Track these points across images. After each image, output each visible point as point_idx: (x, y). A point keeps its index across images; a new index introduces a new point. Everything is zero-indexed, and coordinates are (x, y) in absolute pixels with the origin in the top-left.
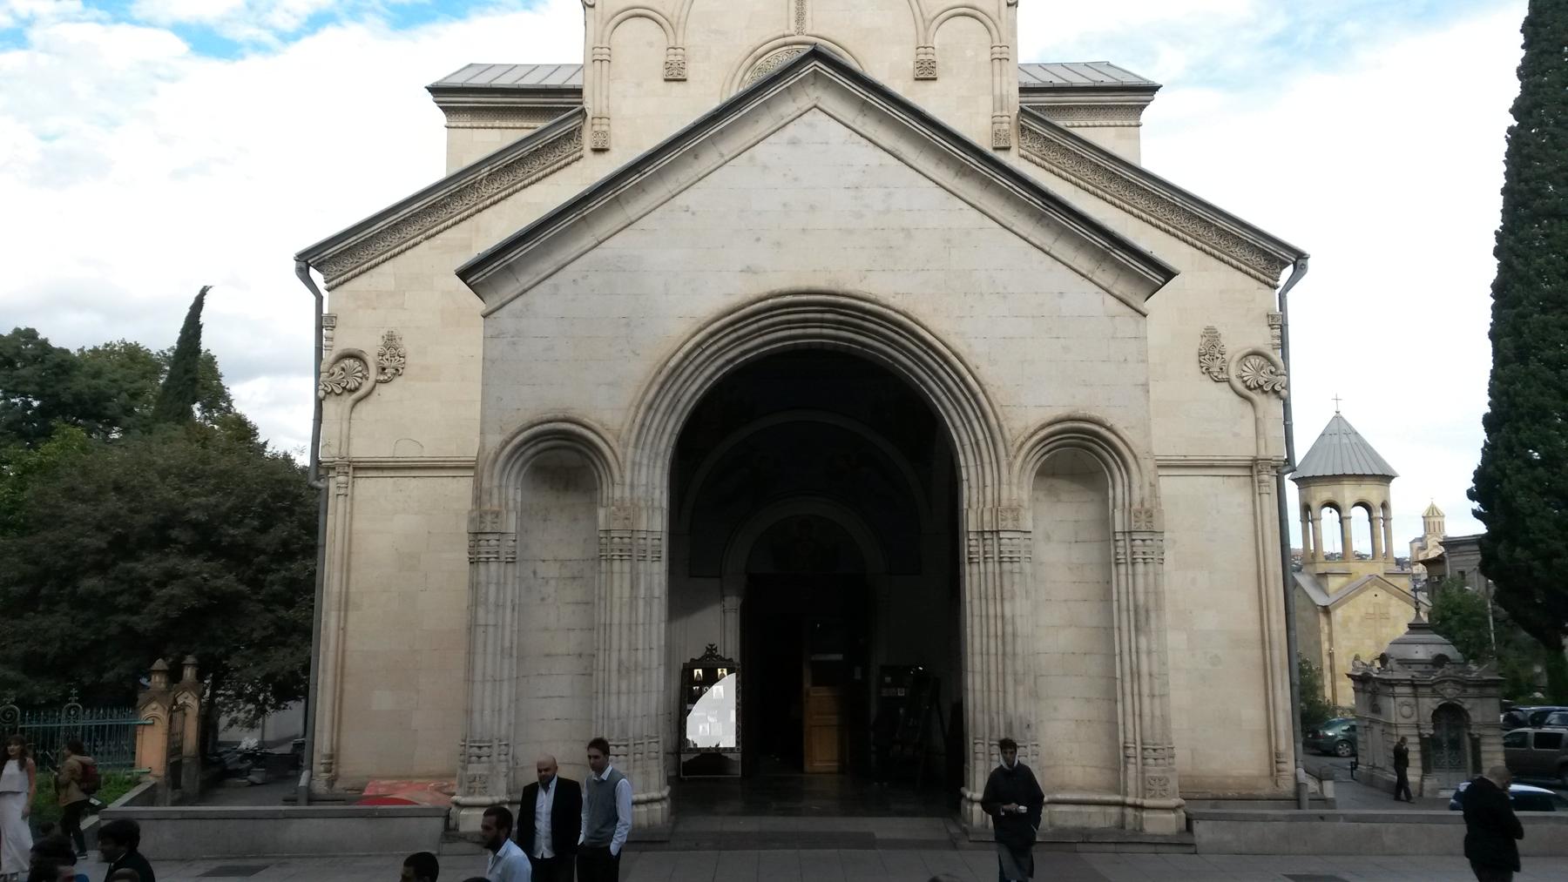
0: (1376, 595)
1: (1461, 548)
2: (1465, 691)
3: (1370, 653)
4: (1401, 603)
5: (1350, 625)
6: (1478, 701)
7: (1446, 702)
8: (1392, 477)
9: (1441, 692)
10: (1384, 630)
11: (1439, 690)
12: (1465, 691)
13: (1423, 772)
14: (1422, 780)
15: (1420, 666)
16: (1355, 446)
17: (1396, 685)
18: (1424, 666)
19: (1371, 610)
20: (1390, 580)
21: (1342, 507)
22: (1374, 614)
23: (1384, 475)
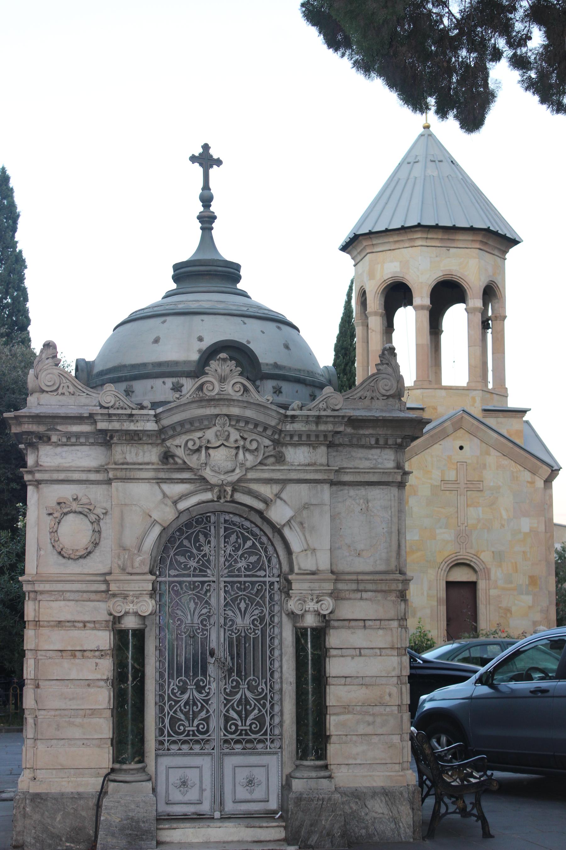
0: (461, 448)
4: (506, 462)
6: (326, 491)
7: (208, 496)
8: (514, 242)
9: (193, 461)
10: (472, 511)
11: (180, 452)
12: (280, 459)
13: (116, 759)
15: (158, 382)
18: (169, 382)
19: (451, 475)
20: (491, 421)
22: (456, 482)
23: (488, 230)
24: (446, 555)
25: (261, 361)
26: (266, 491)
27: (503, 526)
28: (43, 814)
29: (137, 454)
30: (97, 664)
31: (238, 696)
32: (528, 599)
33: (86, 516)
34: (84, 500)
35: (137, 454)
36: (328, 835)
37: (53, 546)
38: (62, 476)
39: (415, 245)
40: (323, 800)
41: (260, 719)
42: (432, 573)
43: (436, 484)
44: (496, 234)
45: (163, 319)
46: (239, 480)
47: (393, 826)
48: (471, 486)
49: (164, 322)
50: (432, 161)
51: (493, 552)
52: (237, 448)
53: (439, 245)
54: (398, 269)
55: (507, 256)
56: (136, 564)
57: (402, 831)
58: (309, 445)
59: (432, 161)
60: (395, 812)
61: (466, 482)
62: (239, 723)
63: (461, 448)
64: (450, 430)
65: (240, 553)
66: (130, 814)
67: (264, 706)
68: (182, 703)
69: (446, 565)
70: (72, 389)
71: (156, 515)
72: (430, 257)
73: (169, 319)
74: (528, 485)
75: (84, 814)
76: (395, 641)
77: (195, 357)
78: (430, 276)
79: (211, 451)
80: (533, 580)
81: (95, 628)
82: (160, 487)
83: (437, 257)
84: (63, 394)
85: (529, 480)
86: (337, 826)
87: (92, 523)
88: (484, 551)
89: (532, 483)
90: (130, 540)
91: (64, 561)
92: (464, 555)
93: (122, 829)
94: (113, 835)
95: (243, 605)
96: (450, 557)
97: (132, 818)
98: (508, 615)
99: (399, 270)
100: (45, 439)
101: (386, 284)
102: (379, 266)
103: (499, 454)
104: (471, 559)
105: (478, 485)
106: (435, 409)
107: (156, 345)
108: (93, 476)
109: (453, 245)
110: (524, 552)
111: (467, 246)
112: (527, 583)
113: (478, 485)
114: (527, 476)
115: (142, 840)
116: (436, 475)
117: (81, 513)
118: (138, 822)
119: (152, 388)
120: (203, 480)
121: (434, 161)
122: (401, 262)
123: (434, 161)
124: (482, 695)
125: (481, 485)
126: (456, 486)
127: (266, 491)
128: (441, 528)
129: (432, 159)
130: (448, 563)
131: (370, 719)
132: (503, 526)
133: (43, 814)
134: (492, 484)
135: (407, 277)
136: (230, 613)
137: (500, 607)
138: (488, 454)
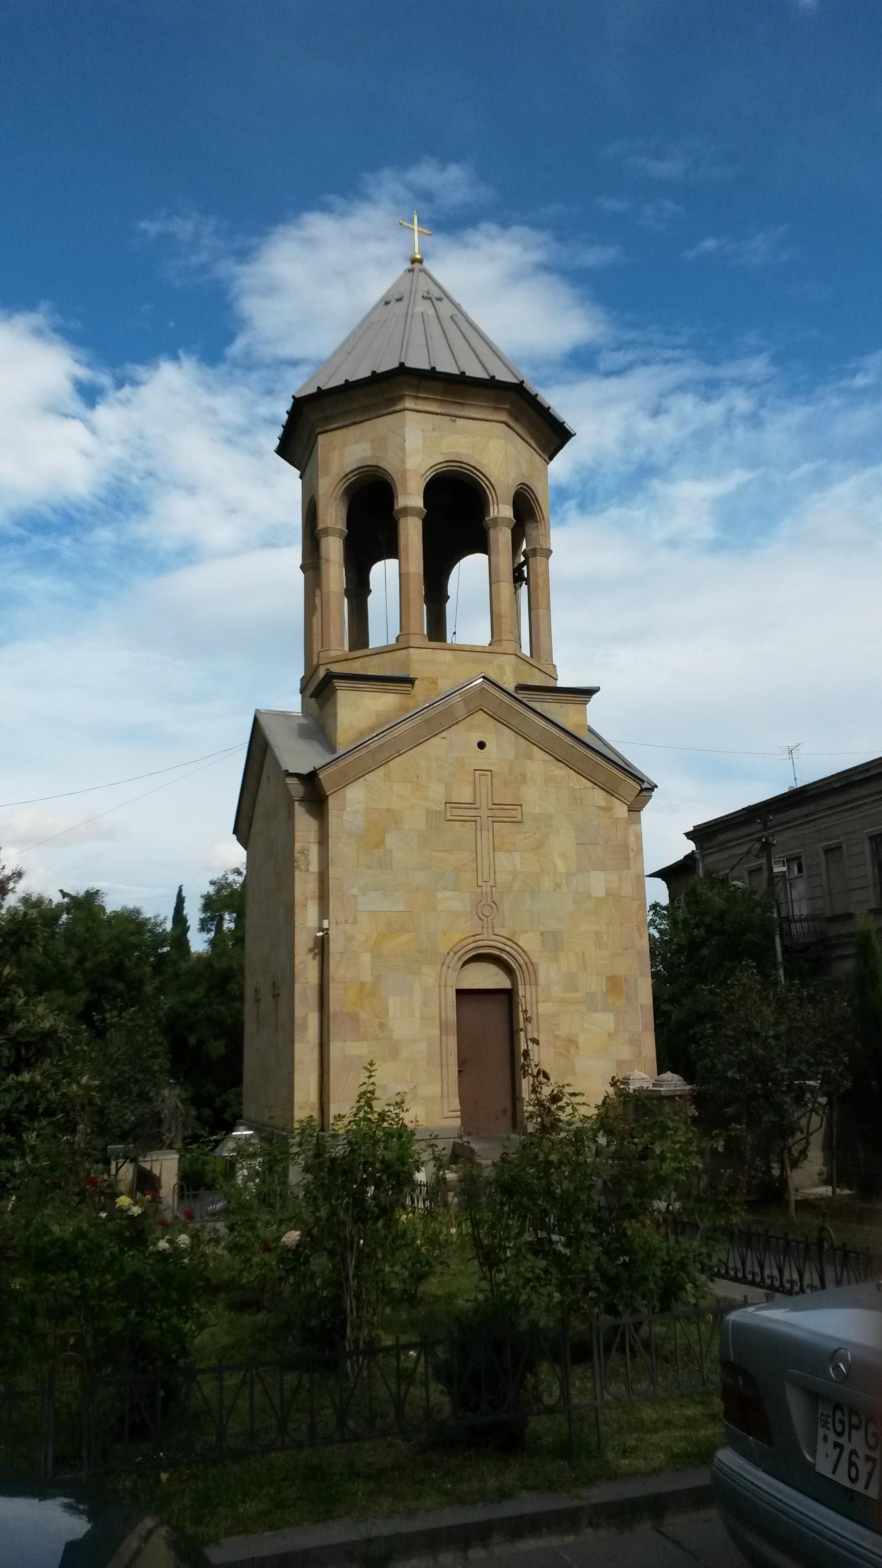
0: (481, 745)
1: (722, 838)
3: (456, 937)
4: (561, 771)
5: (391, 840)
10: (502, 859)
19: (464, 794)
21: (397, 478)
22: (472, 805)
24: (456, 940)
27: (558, 885)
32: (606, 1021)
39: (397, 408)
42: (429, 975)
43: (436, 808)
48: (498, 813)
51: (542, 934)
53: (438, 411)
54: (369, 454)
61: (491, 806)
63: (481, 745)
64: (461, 711)
69: (456, 957)
72: (423, 430)
74: (602, 813)
78: (423, 460)
80: (615, 984)
83: (434, 430)
85: (603, 804)
88: (526, 932)
89: (608, 809)
92: (489, 941)
96: (464, 943)
98: (573, 1050)
101: (349, 481)
102: (337, 451)
104: (502, 946)
105: (513, 813)
106: (434, 682)
109: (462, 414)
110: (596, 933)
111: (485, 417)
112: (604, 989)
113: (513, 813)
114: (598, 797)
116: (437, 792)
121: (430, 299)
125: (520, 812)
126: (473, 813)
128: (445, 889)
130: (459, 954)
132: (558, 885)
134: (537, 811)
135: (383, 465)
137: (557, 1037)
138: (529, 757)
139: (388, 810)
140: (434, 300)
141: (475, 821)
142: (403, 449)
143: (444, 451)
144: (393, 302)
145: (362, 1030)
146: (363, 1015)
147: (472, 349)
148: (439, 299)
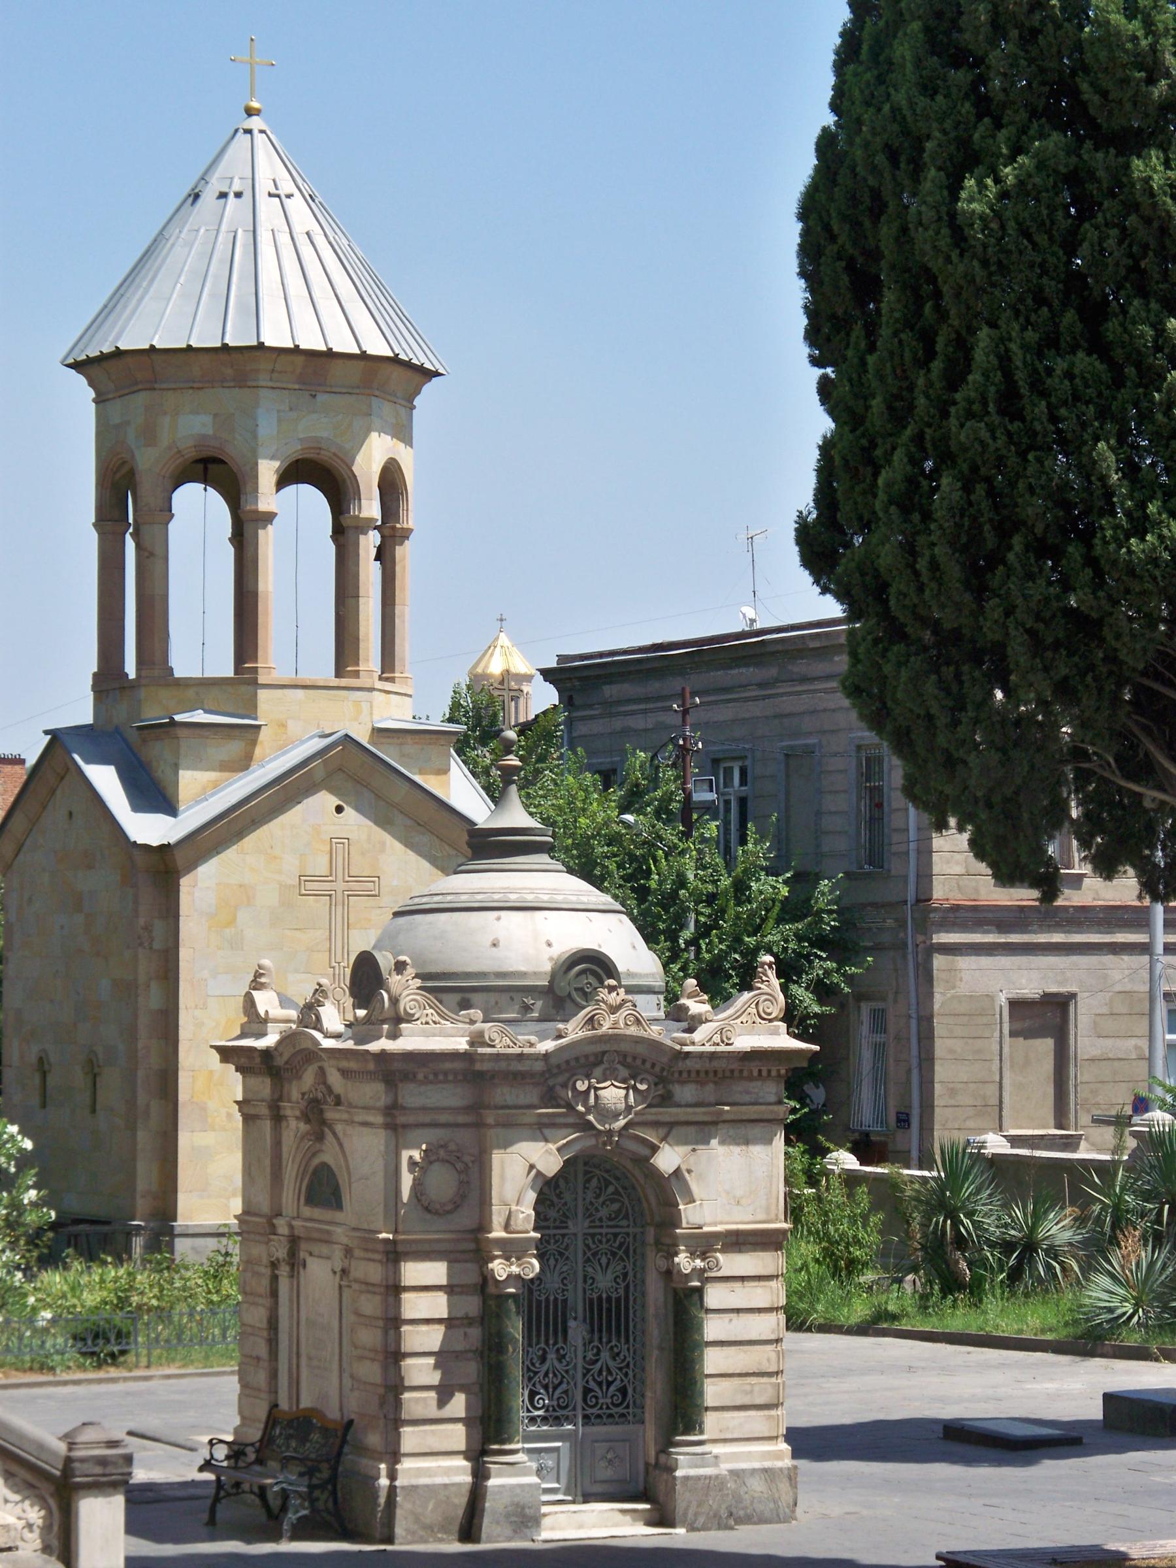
1: (610, 691)
2: (666, 1100)
5: (243, 916)
14: (480, 1474)
16: (302, 241)
17: (409, 1077)
23: (395, 360)
25: (620, 969)
26: (651, 1137)
28: (414, 1503)
29: (517, 1096)
30: (465, 1334)
31: (598, 1365)
33: (454, 1165)
34: (452, 1147)
35: (517, 1096)
36: (715, 1516)
37: (419, 1200)
38: (427, 1119)
40: (710, 1477)
41: (623, 1391)
43: (290, 882)
44: (408, 365)
45: (495, 914)
46: (626, 1127)
47: (772, 1505)
49: (498, 919)
50: (270, 195)
52: (627, 1089)
55: (417, 401)
56: (520, 1222)
57: (781, 1511)
58: (697, 1082)
59: (270, 195)
60: (774, 1490)
62: (600, 1394)
65: (601, 1200)
66: (516, 1500)
67: (626, 1375)
68: (541, 1375)
70: (437, 1018)
71: (540, 1167)
72: (278, 411)
73: (503, 914)
75: (456, 1501)
76: (775, 1299)
77: (547, 967)
79: (600, 1092)
81: (461, 1293)
82: (542, 1133)
83: (291, 409)
84: (427, 1023)
86: (724, 1506)
87: (459, 1172)
90: (510, 1192)
91: (428, 1216)
93: (508, 1516)
94: (498, 1523)
95: (604, 1261)
97: (517, 1505)
99: (211, 432)
100: (411, 1076)
103: (409, 822)
107: (494, 949)
108: (461, 1119)
115: (527, 1527)
116: (290, 866)
117: (447, 1161)
118: (523, 1508)
119: (497, 1003)
120: (589, 1126)
121: (278, 196)
122: (215, 415)
123: (278, 196)
124: (1156, 1391)
127: (651, 1137)
128: (297, 971)
129: (273, 191)
131: (748, 1388)
133: (414, 1503)
134: (395, 883)
136: (590, 1270)
139: (241, 886)
140: (283, 198)
141: (330, 896)
142: (255, 437)
143: (301, 436)
144: (231, 195)
145: (210, 1120)
146: (211, 1105)
147: (336, 296)
148: (289, 196)
